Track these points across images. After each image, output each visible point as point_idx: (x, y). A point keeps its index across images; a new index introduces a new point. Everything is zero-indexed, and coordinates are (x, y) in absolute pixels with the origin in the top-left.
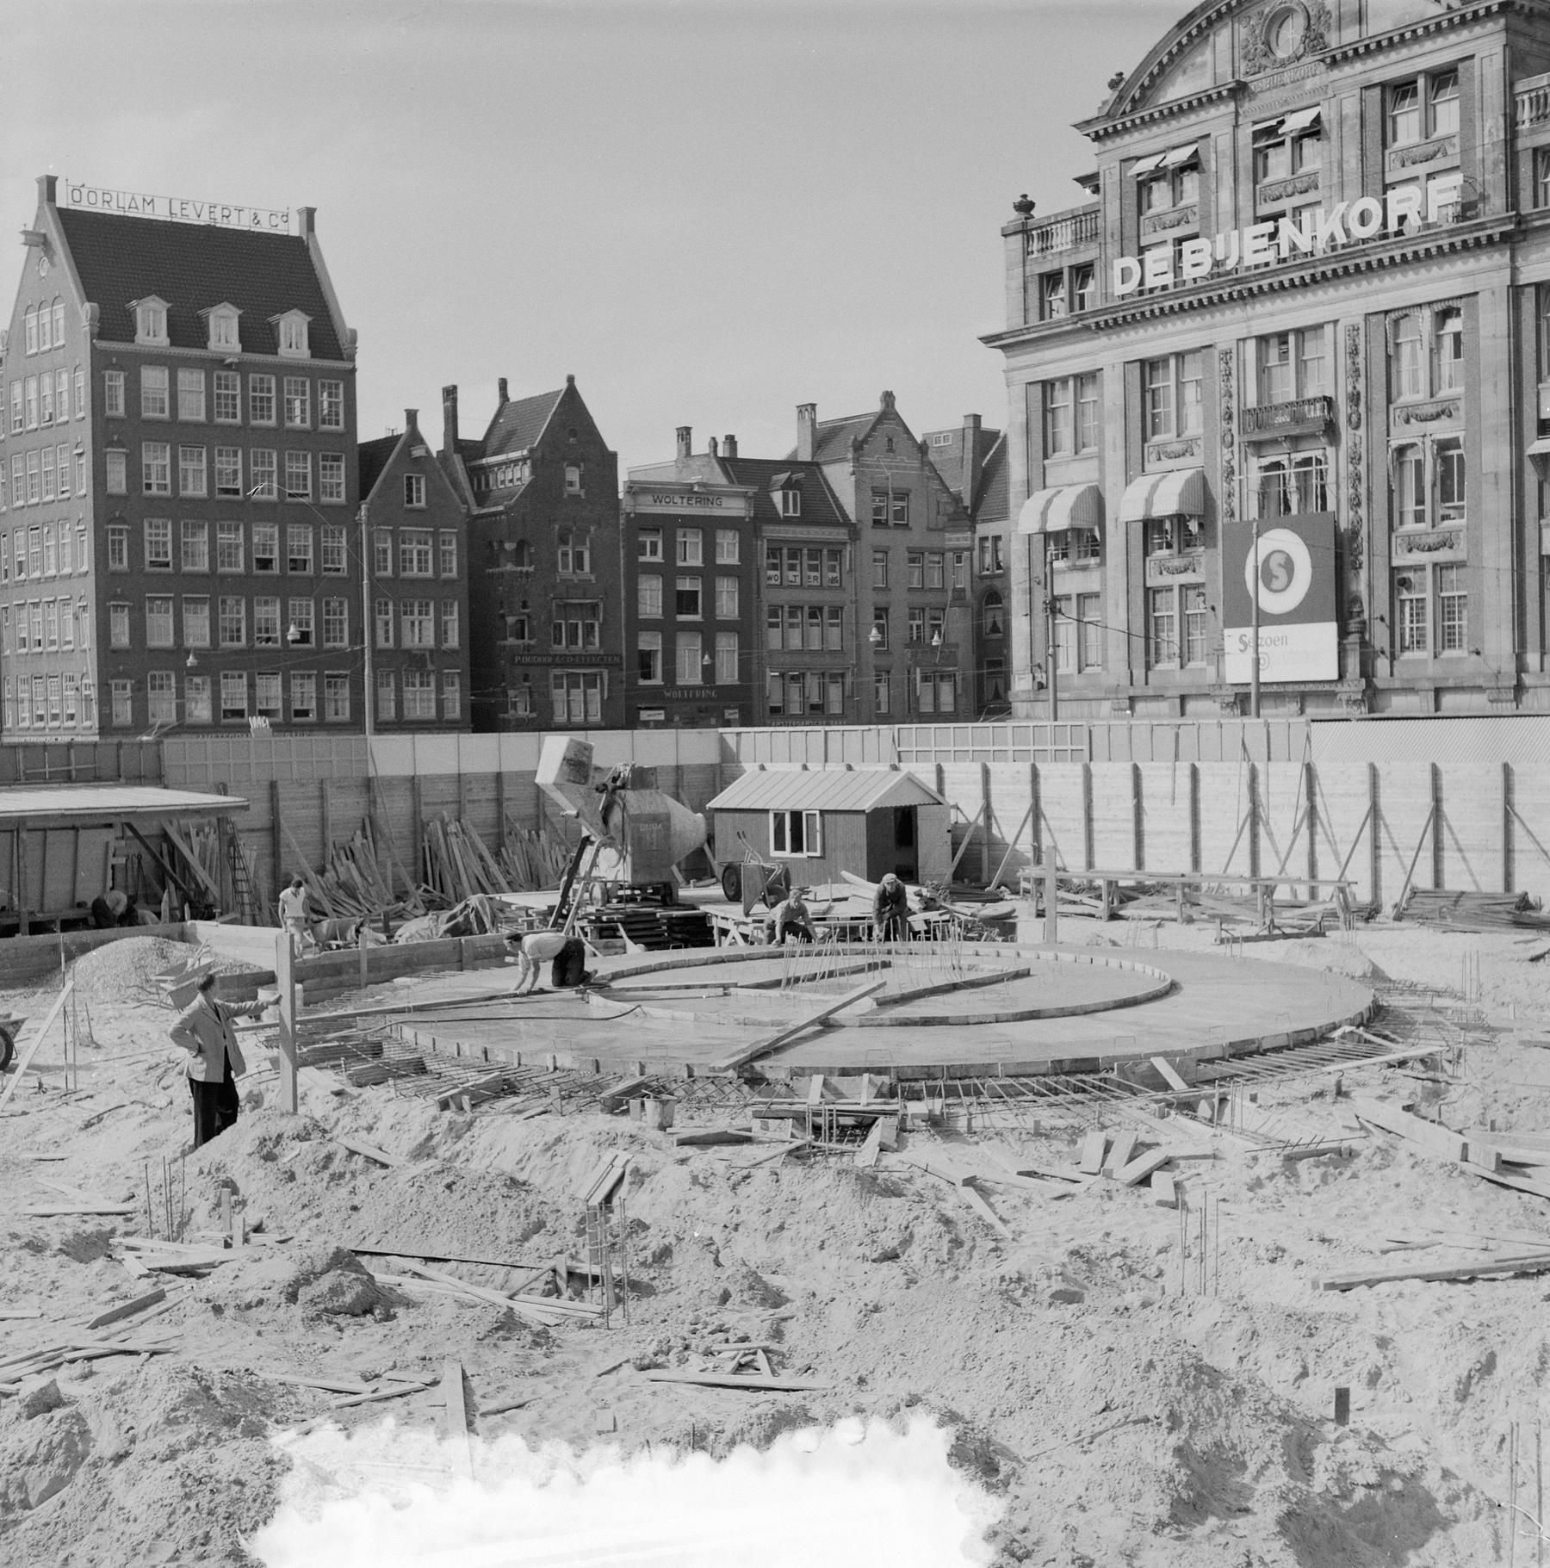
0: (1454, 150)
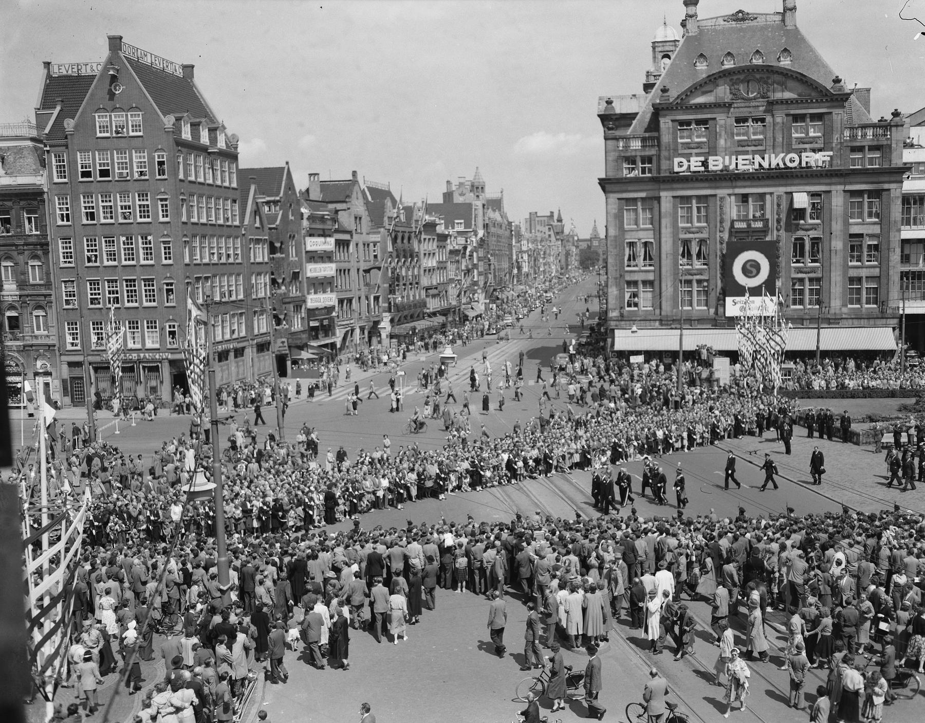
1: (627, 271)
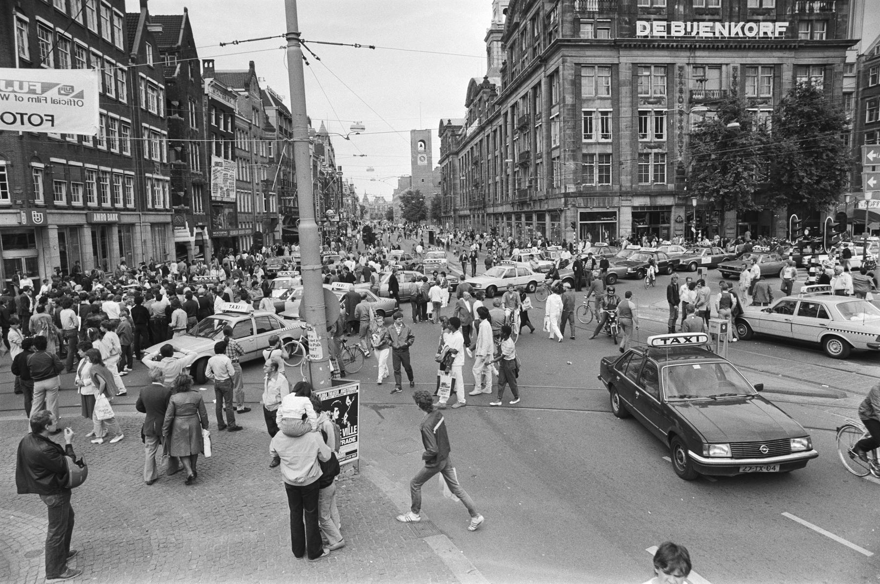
0: (773, 13)
1: (585, 144)
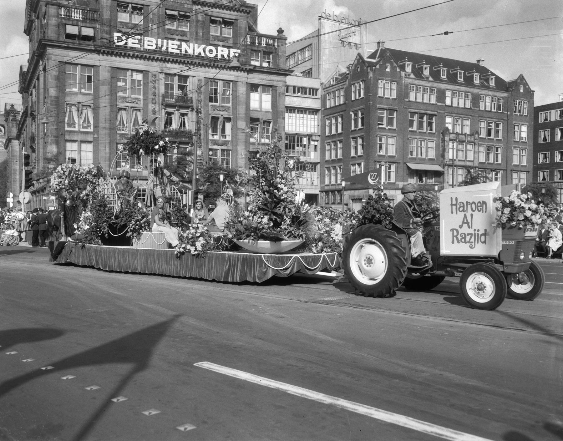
0: (231, 41)
1: (67, 131)
